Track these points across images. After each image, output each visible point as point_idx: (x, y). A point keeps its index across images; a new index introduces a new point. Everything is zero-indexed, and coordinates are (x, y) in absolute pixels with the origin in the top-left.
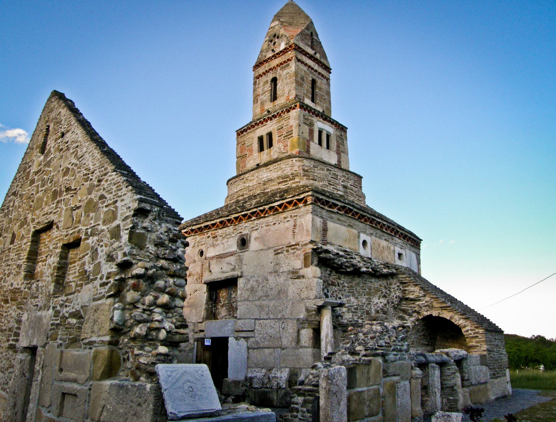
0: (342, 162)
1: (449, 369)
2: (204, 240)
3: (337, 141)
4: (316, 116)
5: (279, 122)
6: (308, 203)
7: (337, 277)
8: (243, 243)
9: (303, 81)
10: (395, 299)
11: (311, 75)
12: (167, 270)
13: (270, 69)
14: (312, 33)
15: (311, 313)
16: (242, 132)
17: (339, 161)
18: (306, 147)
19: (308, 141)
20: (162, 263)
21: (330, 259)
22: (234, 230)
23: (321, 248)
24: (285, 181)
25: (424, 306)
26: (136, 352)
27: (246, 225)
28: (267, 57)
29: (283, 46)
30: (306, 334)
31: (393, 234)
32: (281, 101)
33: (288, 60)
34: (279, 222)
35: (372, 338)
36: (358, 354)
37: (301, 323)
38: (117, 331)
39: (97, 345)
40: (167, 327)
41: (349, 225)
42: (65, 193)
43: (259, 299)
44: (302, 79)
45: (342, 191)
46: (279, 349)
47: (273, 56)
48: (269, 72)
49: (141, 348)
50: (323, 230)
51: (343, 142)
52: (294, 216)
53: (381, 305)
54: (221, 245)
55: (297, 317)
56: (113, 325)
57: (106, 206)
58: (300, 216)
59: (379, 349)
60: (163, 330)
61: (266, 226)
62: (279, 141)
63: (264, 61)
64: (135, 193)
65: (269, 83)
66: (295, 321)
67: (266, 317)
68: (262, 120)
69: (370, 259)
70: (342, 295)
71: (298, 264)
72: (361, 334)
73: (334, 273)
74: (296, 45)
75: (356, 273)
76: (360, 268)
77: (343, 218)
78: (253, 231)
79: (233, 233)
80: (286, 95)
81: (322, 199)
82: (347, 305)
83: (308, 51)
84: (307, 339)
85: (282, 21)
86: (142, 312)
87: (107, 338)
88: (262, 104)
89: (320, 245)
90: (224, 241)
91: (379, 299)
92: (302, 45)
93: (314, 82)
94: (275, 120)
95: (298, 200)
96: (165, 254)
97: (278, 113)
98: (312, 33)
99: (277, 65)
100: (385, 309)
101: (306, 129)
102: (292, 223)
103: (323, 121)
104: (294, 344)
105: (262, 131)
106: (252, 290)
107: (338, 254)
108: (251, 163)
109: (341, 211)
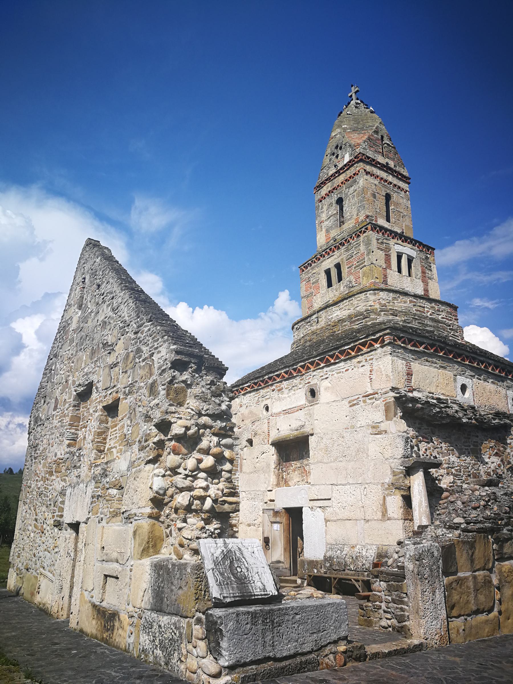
0: (430, 291)
2: (268, 393)
3: (422, 266)
4: (393, 238)
5: (347, 250)
6: (386, 343)
7: (430, 430)
8: (313, 393)
9: (375, 197)
12: (211, 427)
13: (334, 189)
14: (382, 137)
15: (397, 477)
16: (306, 268)
17: (426, 290)
20: (205, 420)
21: (418, 409)
22: (301, 380)
23: (405, 396)
24: (358, 320)
26: (180, 525)
27: (315, 373)
28: (330, 175)
29: (347, 158)
30: (395, 502)
31: (503, 375)
32: (349, 225)
33: (354, 174)
34: (353, 367)
35: (475, 508)
36: (457, 528)
37: (387, 489)
38: (158, 502)
39: (136, 518)
40: (213, 495)
42: (103, 350)
43: (335, 460)
44: (374, 196)
45: (431, 326)
46: (363, 521)
47: (336, 173)
48: (332, 192)
49: (185, 521)
50: (408, 374)
51: (431, 267)
52: (370, 360)
54: (288, 398)
55: (382, 482)
56: (152, 495)
57: (144, 360)
58: (377, 359)
59: (485, 522)
60: (208, 498)
61: (337, 373)
62: (350, 273)
63: (326, 180)
64: (172, 343)
65: (334, 205)
66: (379, 486)
67: (343, 483)
68: (328, 250)
69: (473, 408)
70: (438, 454)
71: (379, 416)
72: (459, 503)
74: (364, 155)
76: (460, 418)
78: (322, 380)
79: (300, 383)
80: (355, 217)
81: (403, 337)
82: (445, 466)
83: (379, 160)
84: (396, 509)
85: (344, 128)
86: (184, 478)
87: (148, 510)
88: (327, 231)
89: (403, 393)
90: (290, 394)
92: (370, 154)
93: (388, 197)
94: (343, 249)
95: (372, 340)
96: (207, 410)
97: (346, 241)
98: (382, 137)
99: (342, 183)
100: (499, 471)
101: (381, 254)
102: (368, 368)
103: (402, 243)
104: (379, 514)
105: (329, 263)
106: (327, 450)
107: (428, 402)
108: (318, 303)
109: (428, 349)
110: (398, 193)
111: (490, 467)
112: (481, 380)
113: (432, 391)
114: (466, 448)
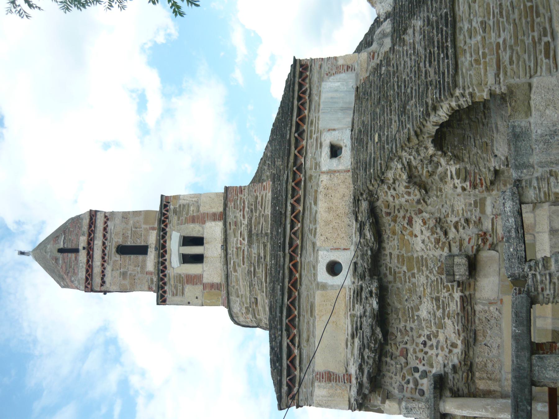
1: (542, 290)
7: (392, 342)
10: (412, 197)
11: (114, 258)
17: (214, 217)
18: (213, 290)
19: (205, 286)
25: (419, 155)
41: (311, 312)
53: (427, 233)
73: (388, 348)
75: (382, 318)
77: (304, 327)
81: (288, 385)
91: (416, 236)
110: (111, 233)
111: (428, 237)
112: (316, 229)
113: (344, 342)
114: (408, 280)
